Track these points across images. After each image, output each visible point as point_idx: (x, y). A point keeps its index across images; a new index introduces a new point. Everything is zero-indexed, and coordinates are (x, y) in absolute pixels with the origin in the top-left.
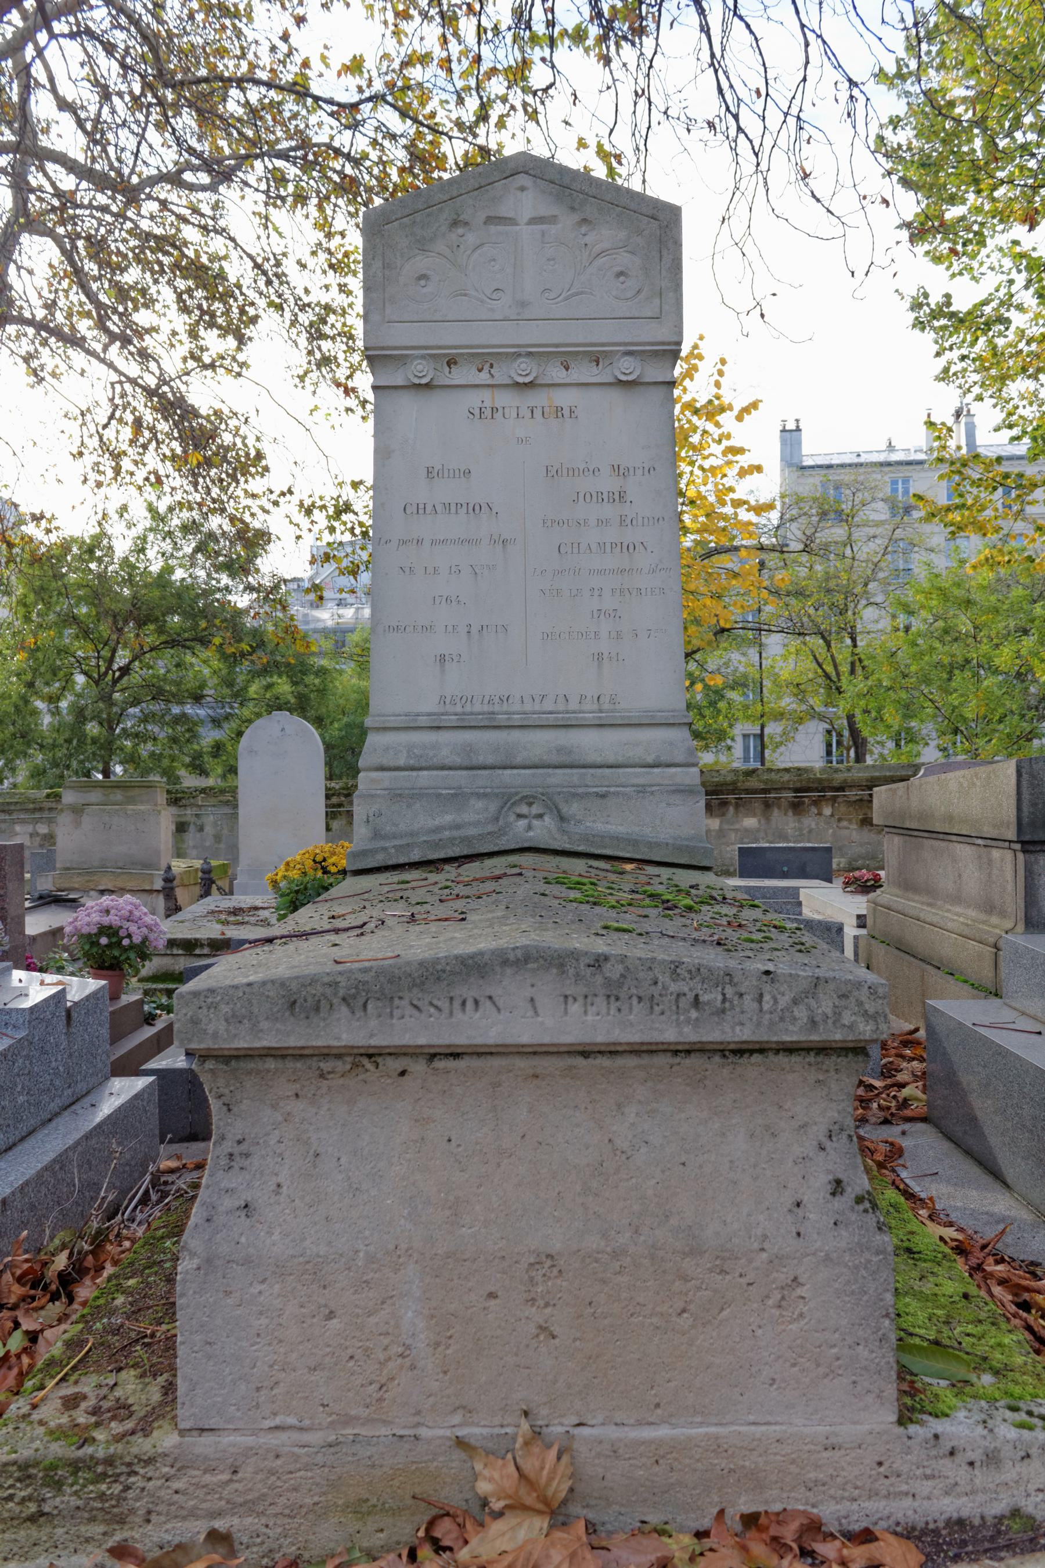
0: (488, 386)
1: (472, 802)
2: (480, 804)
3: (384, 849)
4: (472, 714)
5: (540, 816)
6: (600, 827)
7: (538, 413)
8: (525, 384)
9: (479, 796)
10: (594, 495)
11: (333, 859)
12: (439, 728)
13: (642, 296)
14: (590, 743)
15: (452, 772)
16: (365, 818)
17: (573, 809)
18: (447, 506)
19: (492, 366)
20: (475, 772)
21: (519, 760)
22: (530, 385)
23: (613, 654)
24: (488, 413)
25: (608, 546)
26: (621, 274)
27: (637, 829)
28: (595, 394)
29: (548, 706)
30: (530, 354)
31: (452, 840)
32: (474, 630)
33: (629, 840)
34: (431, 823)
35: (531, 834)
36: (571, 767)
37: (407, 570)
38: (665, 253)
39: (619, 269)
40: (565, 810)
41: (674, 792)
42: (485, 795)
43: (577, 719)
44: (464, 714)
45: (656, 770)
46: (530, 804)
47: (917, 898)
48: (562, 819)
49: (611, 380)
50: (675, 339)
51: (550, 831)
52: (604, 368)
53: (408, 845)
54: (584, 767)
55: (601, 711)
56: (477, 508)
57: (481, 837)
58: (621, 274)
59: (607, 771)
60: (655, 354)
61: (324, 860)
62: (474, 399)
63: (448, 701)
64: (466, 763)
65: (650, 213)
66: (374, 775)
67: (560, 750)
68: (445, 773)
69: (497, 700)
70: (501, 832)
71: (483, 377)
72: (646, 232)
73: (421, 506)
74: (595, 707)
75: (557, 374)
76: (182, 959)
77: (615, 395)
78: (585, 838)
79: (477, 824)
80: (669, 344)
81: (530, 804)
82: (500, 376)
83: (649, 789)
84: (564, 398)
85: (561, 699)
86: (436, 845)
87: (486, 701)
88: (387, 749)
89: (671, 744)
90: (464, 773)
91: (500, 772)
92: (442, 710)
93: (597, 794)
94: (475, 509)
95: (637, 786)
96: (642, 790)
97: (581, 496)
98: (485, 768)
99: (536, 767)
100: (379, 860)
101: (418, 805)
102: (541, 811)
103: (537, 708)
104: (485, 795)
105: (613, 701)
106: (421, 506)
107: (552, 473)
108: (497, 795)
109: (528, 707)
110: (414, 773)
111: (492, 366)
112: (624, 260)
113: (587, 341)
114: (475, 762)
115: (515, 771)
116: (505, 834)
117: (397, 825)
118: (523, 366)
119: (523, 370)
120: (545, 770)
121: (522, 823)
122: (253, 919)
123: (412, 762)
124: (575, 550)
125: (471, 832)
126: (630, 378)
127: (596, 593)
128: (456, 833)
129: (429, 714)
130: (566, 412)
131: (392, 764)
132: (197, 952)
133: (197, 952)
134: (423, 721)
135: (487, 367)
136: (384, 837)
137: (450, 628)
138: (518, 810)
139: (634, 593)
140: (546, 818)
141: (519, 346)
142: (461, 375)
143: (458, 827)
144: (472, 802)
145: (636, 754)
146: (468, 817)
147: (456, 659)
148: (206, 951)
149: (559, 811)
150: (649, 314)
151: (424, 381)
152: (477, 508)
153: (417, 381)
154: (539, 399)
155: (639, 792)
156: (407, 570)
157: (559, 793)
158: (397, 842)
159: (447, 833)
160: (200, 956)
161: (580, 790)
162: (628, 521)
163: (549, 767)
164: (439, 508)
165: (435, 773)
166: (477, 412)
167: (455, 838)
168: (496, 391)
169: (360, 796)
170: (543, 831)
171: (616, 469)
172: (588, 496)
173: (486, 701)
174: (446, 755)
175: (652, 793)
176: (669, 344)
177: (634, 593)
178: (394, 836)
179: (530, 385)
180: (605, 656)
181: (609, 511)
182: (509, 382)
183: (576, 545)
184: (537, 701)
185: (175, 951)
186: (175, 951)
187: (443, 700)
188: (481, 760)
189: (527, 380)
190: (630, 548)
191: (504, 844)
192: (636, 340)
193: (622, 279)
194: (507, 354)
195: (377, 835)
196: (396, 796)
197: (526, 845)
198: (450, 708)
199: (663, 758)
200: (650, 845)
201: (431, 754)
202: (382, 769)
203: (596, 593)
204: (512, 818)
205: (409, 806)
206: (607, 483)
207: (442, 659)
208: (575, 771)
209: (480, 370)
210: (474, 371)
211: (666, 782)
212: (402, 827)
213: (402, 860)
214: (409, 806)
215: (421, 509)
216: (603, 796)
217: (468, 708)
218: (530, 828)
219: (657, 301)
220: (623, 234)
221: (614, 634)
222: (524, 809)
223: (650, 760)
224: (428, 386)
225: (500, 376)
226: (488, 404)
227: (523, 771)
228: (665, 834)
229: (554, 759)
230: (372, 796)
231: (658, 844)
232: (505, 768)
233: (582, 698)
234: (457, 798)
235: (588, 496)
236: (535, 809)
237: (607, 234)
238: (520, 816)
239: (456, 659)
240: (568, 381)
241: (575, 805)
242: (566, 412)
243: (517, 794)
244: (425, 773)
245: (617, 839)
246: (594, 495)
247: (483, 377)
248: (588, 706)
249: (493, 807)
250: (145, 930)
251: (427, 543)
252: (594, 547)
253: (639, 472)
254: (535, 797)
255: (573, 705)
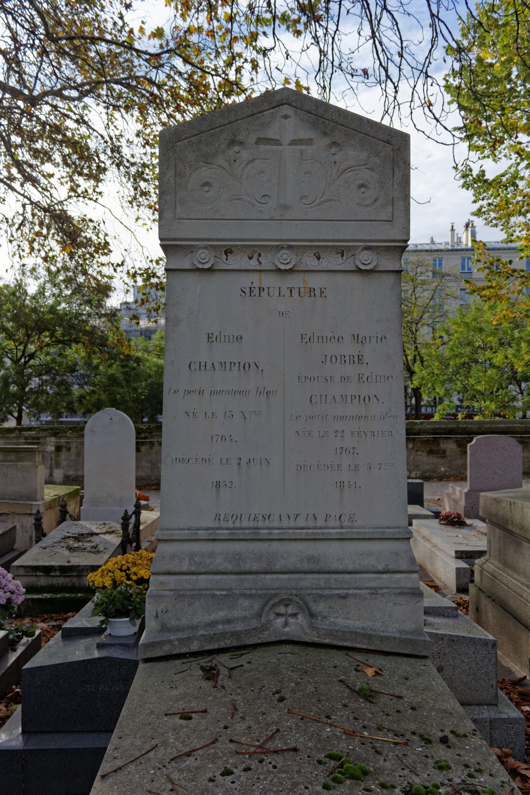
0: (257, 271)
1: (241, 601)
2: (246, 603)
3: (170, 641)
4: (241, 528)
5: (294, 615)
6: (341, 622)
7: (295, 293)
8: (285, 270)
9: (246, 596)
10: (339, 357)
11: (134, 569)
12: (214, 540)
13: (378, 203)
14: (333, 553)
15: (224, 577)
16: (154, 614)
17: (320, 607)
18: (223, 364)
19: (260, 255)
20: (243, 577)
21: (277, 567)
22: (291, 271)
23: (352, 483)
24: (256, 291)
25: (349, 398)
26: (362, 186)
27: (370, 624)
28: (340, 278)
29: (301, 522)
30: (290, 247)
31: (224, 635)
32: (244, 462)
33: (364, 635)
34: (208, 618)
35: (287, 629)
36: (319, 572)
37: (191, 414)
38: (396, 170)
39: (361, 182)
40: (314, 608)
41: (400, 594)
42: (251, 596)
43: (323, 534)
44: (234, 529)
45: (385, 576)
46: (287, 606)
47: (516, 576)
48: (312, 615)
49: (353, 268)
50: (405, 238)
51: (302, 627)
52: (347, 259)
53: (189, 638)
54: (329, 572)
55: (342, 527)
56: (247, 366)
57: (248, 632)
58: (362, 186)
59: (347, 576)
60: (388, 249)
61: (128, 569)
62: (246, 280)
63: (222, 518)
64: (236, 569)
65: (385, 139)
66: (162, 578)
67: (310, 559)
68: (219, 577)
69: (260, 517)
70: (264, 628)
71: (253, 264)
72: (382, 154)
73: (203, 364)
74: (337, 524)
75: (309, 261)
76: (42, 579)
77: (356, 279)
78: (330, 633)
79: (244, 619)
80: (398, 241)
81: (287, 606)
82: (267, 262)
83: (380, 592)
84: (316, 281)
85: (311, 517)
86: (211, 638)
87: (252, 519)
88: (173, 557)
89: (397, 554)
90: (234, 577)
91: (263, 576)
92: (217, 525)
93: (340, 596)
94: (245, 367)
95: (371, 588)
96: (374, 591)
97: (328, 358)
98: (251, 573)
99: (291, 572)
100: (165, 650)
101: (197, 604)
102: (295, 611)
103: (292, 524)
104: (251, 596)
105: (351, 519)
106: (203, 364)
107: (306, 340)
108: (260, 596)
109: (285, 523)
110: (194, 577)
111: (260, 255)
112: (365, 175)
113: (336, 238)
114: (243, 569)
115: (275, 576)
116: (267, 629)
117: (180, 620)
118: (285, 256)
119: (285, 259)
120: (298, 576)
121: (280, 621)
122: (88, 545)
123: (193, 568)
124: (323, 401)
125: (239, 627)
126: (368, 268)
127: (339, 434)
128: (228, 628)
129: (207, 529)
130: (318, 293)
131: (177, 570)
132: (52, 574)
133: (52, 574)
134: (202, 534)
135: (256, 256)
136: (170, 630)
137: (224, 461)
138: (277, 611)
139: (369, 435)
140: (299, 617)
141: (281, 240)
142: (236, 261)
143: (229, 621)
144: (241, 601)
145: (369, 562)
146: (236, 613)
147: (229, 485)
148: (58, 573)
149: (309, 609)
150: (384, 218)
151: (206, 266)
152: (247, 366)
153: (200, 266)
154: (295, 281)
155: (372, 594)
156: (191, 414)
157: (309, 595)
158: (181, 635)
159: (220, 627)
160: (53, 576)
161: (327, 592)
162: (365, 379)
163: (301, 572)
164: (217, 366)
165: (211, 577)
166: (247, 291)
167: (226, 633)
168: (262, 274)
169: (151, 596)
170: (297, 627)
171: (356, 337)
172: (334, 358)
173: (252, 519)
174: (220, 563)
175: (382, 595)
176: (398, 241)
177: (369, 435)
178: (178, 629)
179: (291, 271)
180: (346, 484)
181: (350, 370)
182: (273, 268)
183: (323, 397)
184: (292, 518)
185: (38, 574)
186: (38, 574)
187: (218, 517)
188: (248, 566)
189: (288, 267)
190: (367, 399)
191: (266, 637)
192: (373, 238)
193: (363, 189)
194: (272, 246)
195: (164, 628)
196: (179, 595)
197: (283, 638)
198: (223, 524)
199: (391, 567)
200: (382, 639)
201: (208, 562)
202: (169, 573)
203: (339, 434)
204: (272, 616)
205: (190, 604)
206: (349, 349)
207: (218, 485)
208: (322, 576)
209: (251, 258)
210: (246, 258)
211: (393, 585)
212: (185, 621)
213: (184, 650)
214: (190, 604)
215: (203, 366)
216: (344, 597)
217: (238, 524)
218: (286, 624)
219: (390, 208)
220: (364, 155)
221: (353, 467)
222: (282, 610)
223: (380, 568)
224: (210, 270)
225: (267, 262)
226: (256, 284)
227: (281, 576)
228: (392, 629)
229: (306, 566)
230: (161, 596)
231: (388, 638)
232: (266, 573)
233: (327, 517)
234: (229, 597)
235: (334, 358)
236: (290, 610)
237: (352, 154)
238: (278, 615)
239: (229, 485)
240: (319, 268)
241: (322, 604)
242: (318, 293)
243: (276, 595)
244: (203, 577)
245: (355, 634)
246: (339, 357)
247: (253, 264)
248: (332, 523)
249: (257, 606)
250: (9, 594)
251: (207, 393)
252: (338, 398)
253: (374, 340)
254: (291, 600)
255: (320, 523)
